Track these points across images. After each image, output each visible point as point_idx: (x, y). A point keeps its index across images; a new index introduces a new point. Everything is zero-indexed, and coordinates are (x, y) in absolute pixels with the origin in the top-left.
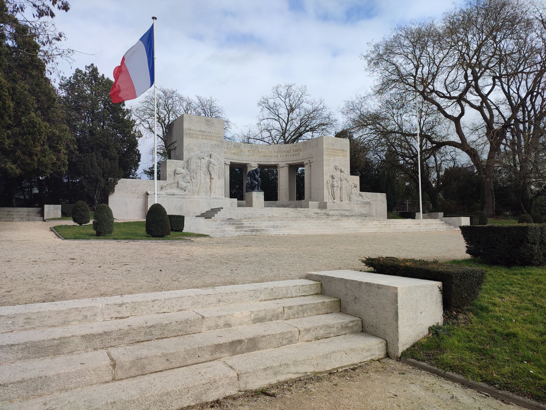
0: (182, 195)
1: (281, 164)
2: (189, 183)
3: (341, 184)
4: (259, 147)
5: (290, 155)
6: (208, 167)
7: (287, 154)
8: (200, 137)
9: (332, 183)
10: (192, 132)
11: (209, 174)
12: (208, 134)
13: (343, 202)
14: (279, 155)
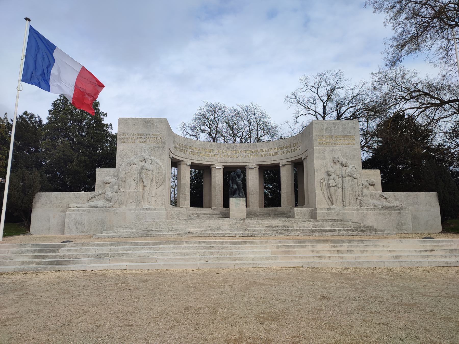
0: (106, 207)
1: (282, 163)
3: (343, 183)
4: (257, 146)
5: (290, 151)
6: (140, 173)
7: (288, 150)
8: (137, 141)
9: (328, 181)
10: (127, 136)
11: (142, 181)
12: (147, 137)
13: (347, 208)
14: (279, 153)
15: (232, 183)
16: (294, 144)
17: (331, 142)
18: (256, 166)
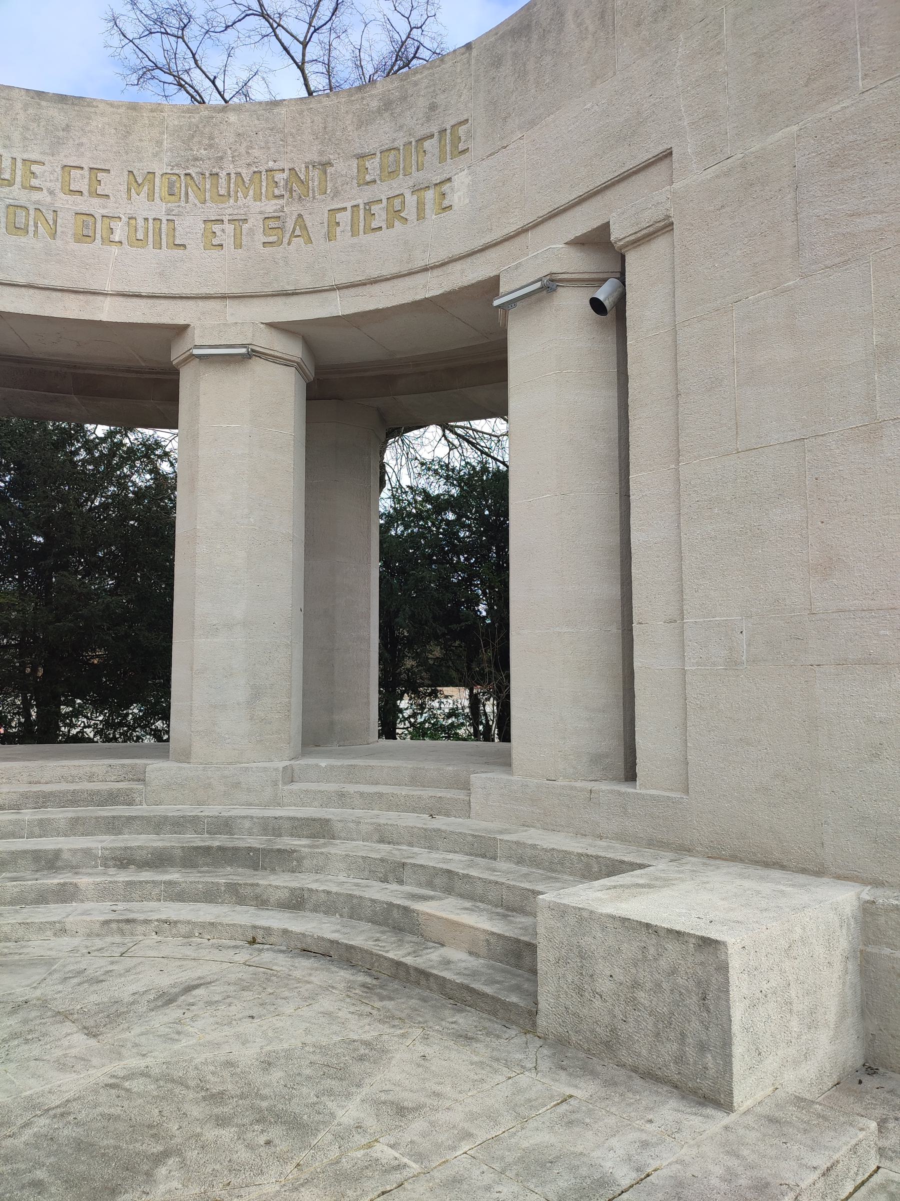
5: (316, 221)
16: (373, 165)
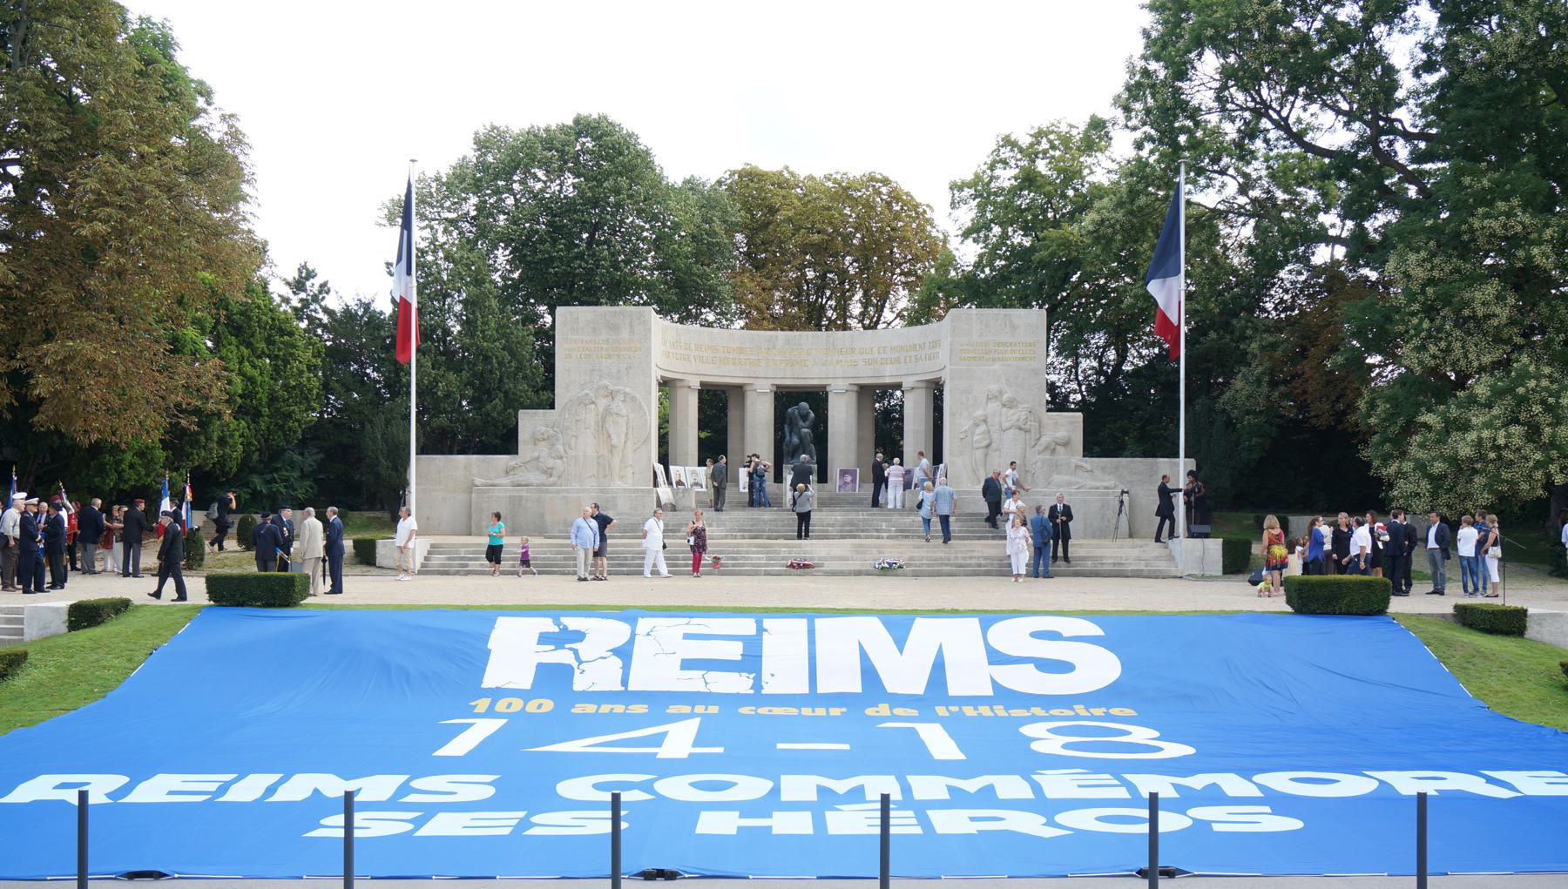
2: (561, 458)
15: (791, 432)
17: (986, 356)
18: (849, 388)
